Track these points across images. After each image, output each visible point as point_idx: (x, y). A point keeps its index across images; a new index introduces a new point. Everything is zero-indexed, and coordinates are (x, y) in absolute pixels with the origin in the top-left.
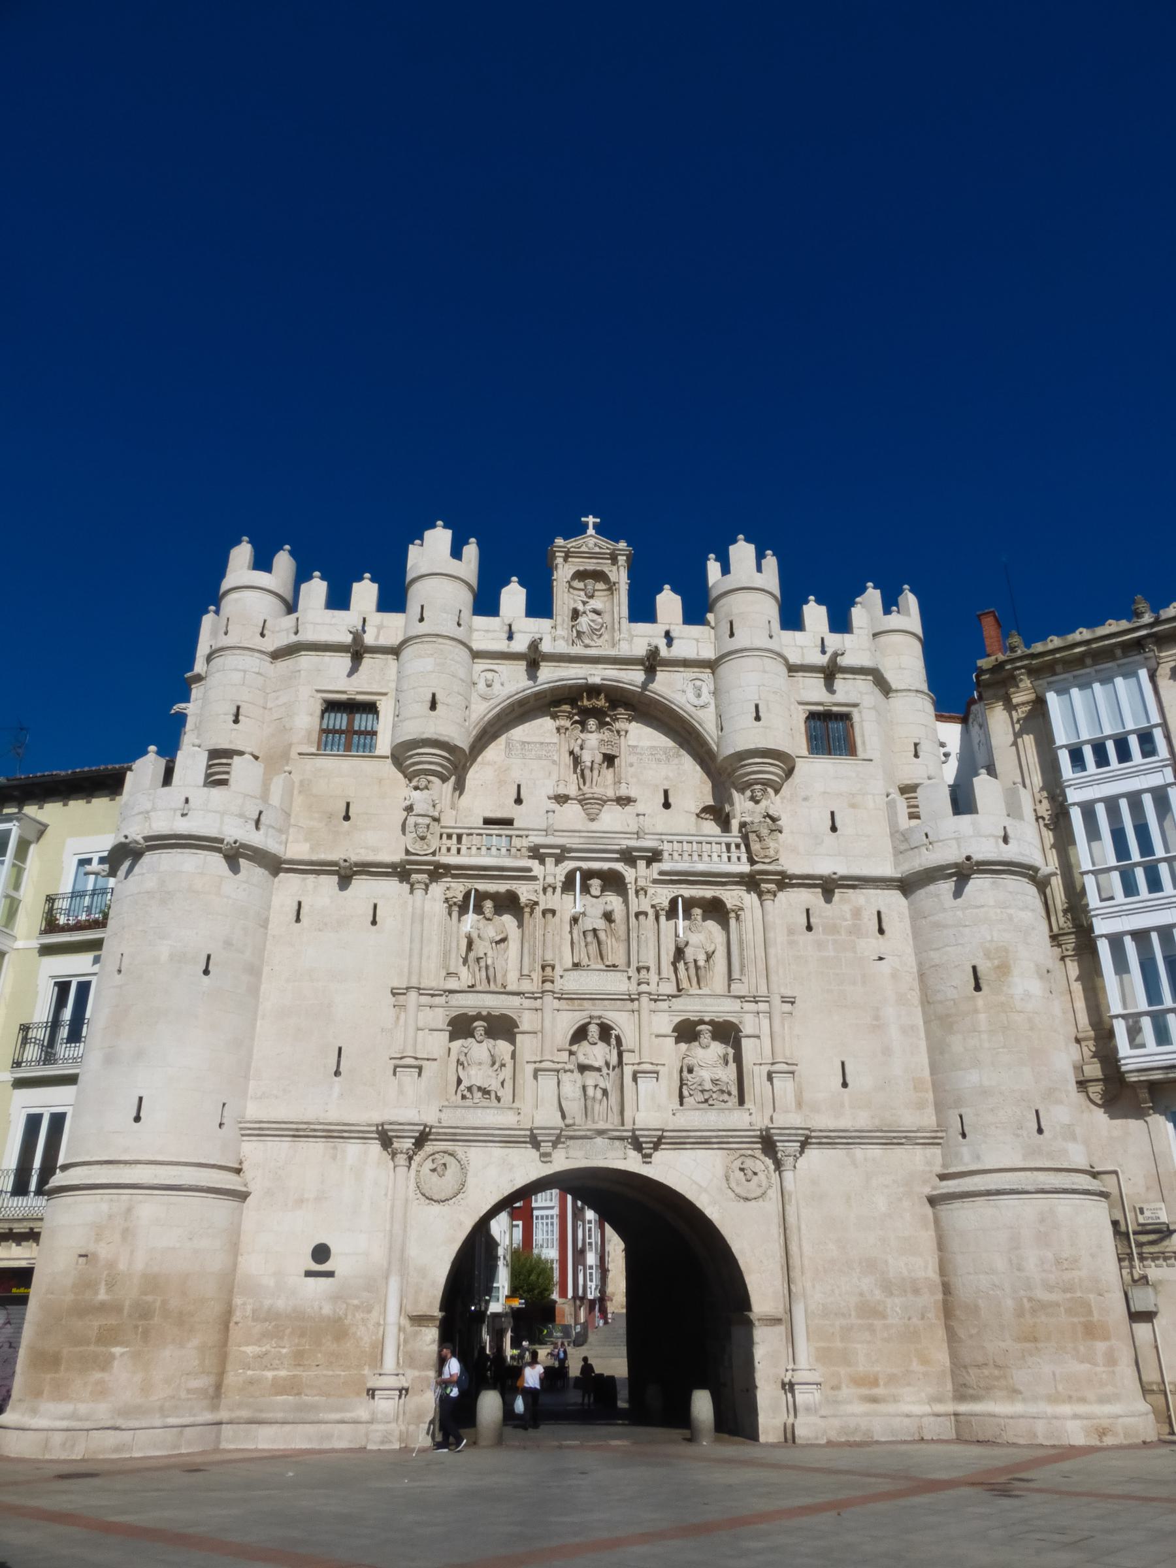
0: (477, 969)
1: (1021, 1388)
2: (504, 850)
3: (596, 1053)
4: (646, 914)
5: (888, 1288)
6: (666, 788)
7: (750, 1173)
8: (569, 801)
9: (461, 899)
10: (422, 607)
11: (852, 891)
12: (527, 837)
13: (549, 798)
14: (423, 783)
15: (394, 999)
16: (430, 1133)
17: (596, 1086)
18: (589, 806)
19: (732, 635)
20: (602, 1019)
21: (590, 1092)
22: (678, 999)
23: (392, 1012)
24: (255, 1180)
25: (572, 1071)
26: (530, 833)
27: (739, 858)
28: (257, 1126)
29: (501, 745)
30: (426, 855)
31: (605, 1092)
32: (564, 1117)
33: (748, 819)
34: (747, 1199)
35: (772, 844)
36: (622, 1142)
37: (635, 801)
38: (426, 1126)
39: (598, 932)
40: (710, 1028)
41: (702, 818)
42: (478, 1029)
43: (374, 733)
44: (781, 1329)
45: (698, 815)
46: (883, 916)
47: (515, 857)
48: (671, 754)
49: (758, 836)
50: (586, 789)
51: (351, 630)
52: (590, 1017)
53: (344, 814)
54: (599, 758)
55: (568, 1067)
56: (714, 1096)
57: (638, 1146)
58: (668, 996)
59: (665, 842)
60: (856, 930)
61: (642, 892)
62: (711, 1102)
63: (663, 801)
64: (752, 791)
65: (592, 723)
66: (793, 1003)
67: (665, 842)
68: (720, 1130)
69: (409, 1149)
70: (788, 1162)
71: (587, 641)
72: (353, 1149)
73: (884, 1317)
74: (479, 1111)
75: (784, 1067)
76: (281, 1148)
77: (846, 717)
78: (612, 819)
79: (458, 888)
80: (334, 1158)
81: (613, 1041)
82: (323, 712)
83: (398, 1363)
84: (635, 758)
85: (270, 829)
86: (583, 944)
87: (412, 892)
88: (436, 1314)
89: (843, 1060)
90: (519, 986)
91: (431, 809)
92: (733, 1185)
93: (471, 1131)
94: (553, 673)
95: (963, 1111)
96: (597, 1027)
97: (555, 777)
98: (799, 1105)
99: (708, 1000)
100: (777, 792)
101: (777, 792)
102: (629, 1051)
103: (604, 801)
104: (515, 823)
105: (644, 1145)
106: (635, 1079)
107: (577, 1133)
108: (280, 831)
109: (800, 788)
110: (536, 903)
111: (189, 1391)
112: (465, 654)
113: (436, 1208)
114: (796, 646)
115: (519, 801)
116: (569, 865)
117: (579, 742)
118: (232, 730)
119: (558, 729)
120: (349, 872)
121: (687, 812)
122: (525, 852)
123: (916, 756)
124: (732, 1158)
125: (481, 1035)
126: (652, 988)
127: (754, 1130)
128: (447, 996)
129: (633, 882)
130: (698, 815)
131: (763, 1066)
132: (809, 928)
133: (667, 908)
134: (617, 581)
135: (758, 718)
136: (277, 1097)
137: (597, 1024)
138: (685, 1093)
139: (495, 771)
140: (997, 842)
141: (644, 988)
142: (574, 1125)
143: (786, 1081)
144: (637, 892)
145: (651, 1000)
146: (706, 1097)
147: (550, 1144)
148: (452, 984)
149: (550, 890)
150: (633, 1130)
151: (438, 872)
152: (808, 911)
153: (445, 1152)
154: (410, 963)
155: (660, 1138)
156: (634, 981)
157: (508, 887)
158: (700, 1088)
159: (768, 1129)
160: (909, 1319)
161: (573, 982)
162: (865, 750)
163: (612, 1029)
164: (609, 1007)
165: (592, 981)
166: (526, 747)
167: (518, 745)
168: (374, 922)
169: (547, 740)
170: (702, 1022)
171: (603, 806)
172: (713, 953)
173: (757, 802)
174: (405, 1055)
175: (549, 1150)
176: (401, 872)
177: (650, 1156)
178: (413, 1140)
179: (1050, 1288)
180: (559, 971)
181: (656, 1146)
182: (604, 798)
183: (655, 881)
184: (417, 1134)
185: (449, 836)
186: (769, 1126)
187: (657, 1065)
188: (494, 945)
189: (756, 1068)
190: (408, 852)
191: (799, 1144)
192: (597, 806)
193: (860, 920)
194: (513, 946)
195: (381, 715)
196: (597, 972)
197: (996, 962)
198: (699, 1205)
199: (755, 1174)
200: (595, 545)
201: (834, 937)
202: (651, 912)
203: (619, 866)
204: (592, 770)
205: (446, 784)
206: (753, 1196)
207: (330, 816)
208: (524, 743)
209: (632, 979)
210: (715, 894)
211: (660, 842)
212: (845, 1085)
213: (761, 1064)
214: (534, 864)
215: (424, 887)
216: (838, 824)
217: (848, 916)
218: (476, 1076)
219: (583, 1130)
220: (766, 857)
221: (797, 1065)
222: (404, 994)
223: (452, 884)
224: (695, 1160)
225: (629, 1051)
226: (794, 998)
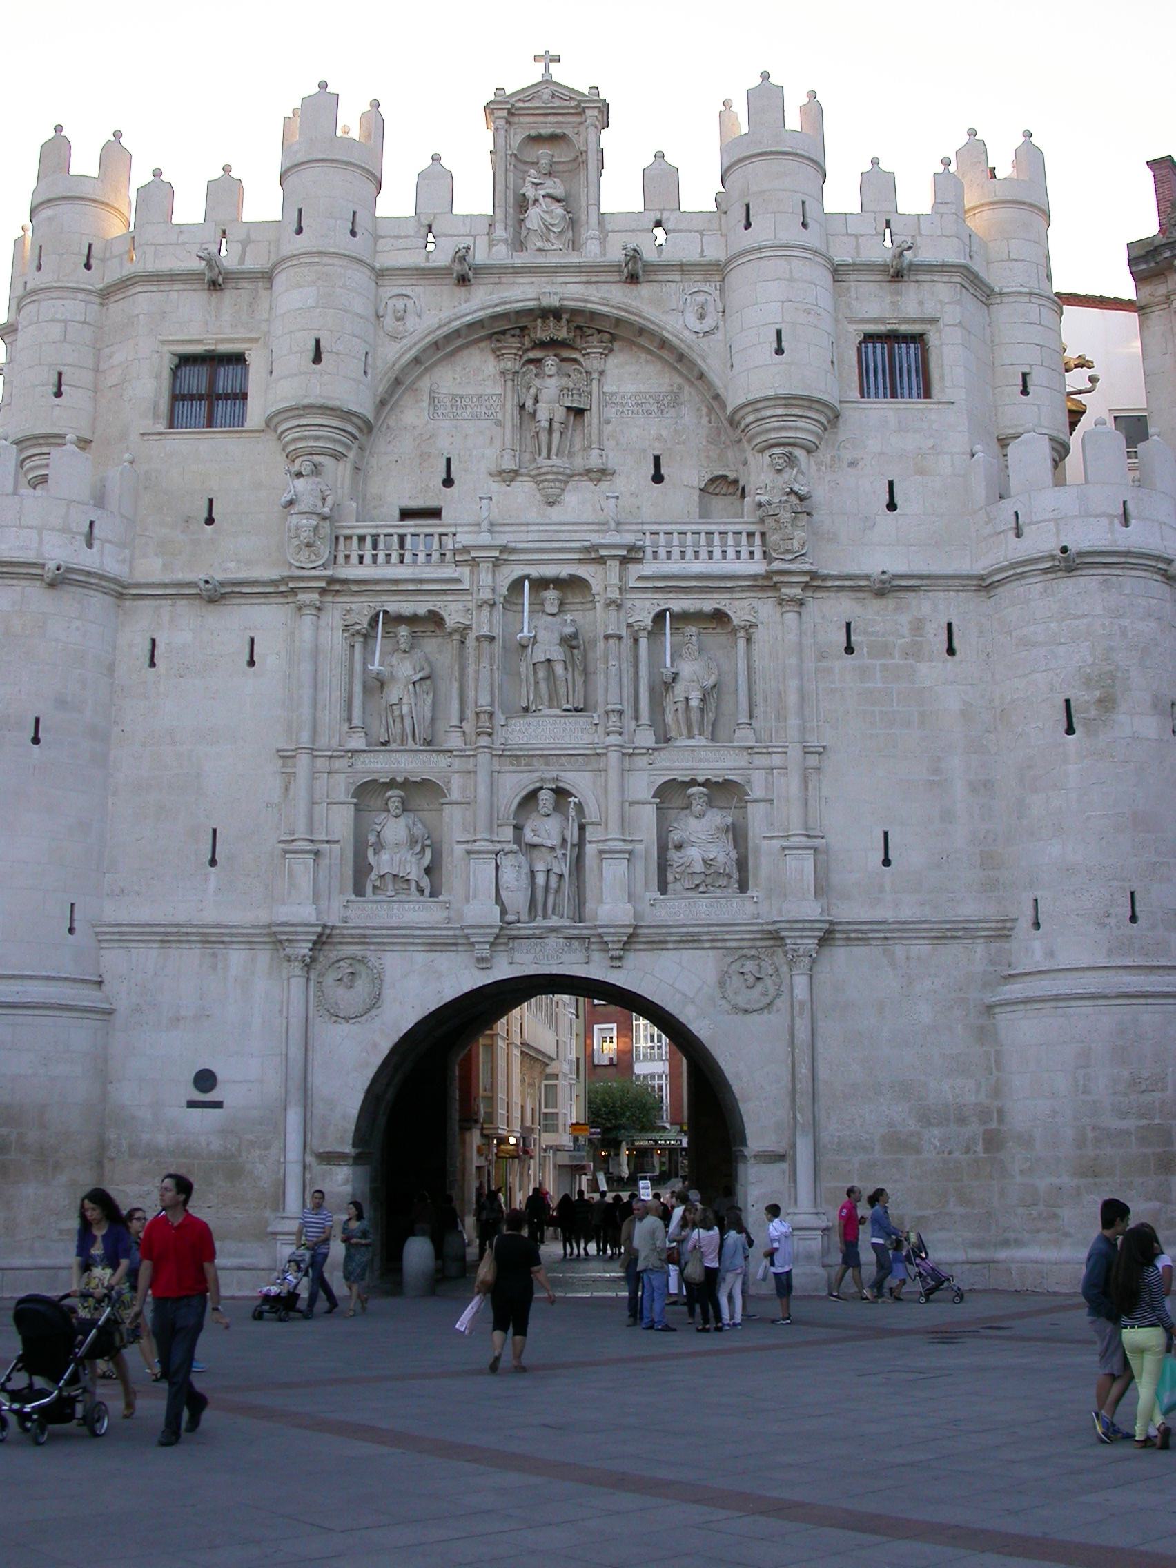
0: (391, 721)
1: (1072, 1231)
2: (422, 557)
4: (620, 638)
5: (926, 1118)
6: (657, 453)
7: (751, 979)
8: (520, 479)
9: (365, 626)
10: (300, 211)
11: (913, 594)
12: (455, 535)
13: (491, 475)
15: (280, 761)
19: (748, 225)
20: (561, 784)
21: (541, 879)
22: (662, 753)
23: (278, 782)
24: (121, 995)
26: (459, 529)
28: (116, 929)
29: (422, 400)
30: (314, 568)
31: (561, 876)
32: (504, 912)
33: (763, 499)
34: (746, 1011)
35: (799, 534)
38: (325, 926)
40: (704, 790)
42: (393, 799)
43: (244, 396)
44: (785, 1166)
46: (955, 629)
48: (665, 402)
49: (777, 521)
51: (200, 254)
52: (542, 780)
53: (205, 515)
54: (560, 414)
55: (507, 847)
56: (709, 880)
58: (648, 749)
59: (648, 534)
60: (915, 652)
62: (701, 889)
63: (652, 472)
65: (551, 363)
66: (820, 754)
67: (648, 534)
69: (304, 956)
70: (802, 964)
71: (539, 244)
72: (236, 957)
73: (918, 1151)
74: (396, 906)
76: (149, 956)
77: (918, 339)
80: (214, 968)
81: (572, 811)
82: (175, 372)
83: (304, 1206)
84: (614, 410)
85: (108, 545)
86: (532, 681)
88: (347, 1151)
89: (886, 829)
92: (730, 993)
93: (384, 932)
94: (491, 294)
95: (1039, 894)
97: (498, 443)
98: (822, 889)
101: (809, 451)
102: (593, 824)
103: (567, 478)
104: (443, 514)
107: (522, 932)
108: (123, 545)
110: (468, 627)
111: (61, 1232)
112: (361, 277)
113: (344, 1027)
114: (848, 234)
115: (448, 482)
117: (533, 391)
118: (53, 407)
119: (503, 373)
123: (1025, 392)
125: (397, 808)
128: (352, 757)
132: (849, 649)
133: (649, 628)
134: (584, 149)
135: (780, 351)
136: (138, 894)
138: (670, 878)
139: (414, 440)
140: (1111, 523)
142: (519, 922)
146: (697, 883)
147: (488, 947)
152: (848, 625)
153: (353, 958)
155: (631, 936)
156: (601, 729)
157: (430, 606)
160: (950, 1153)
162: (943, 390)
163: (571, 795)
164: (569, 767)
166: (459, 403)
167: (446, 400)
168: (251, 663)
169: (489, 391)
170: (693, 783)
171: (566, 482)
174: (295, 837)
175: (486, 954)
179: (1124, 1115)
180: (500, 718)
182: (568, 471)
184: (315, 938)
188: (411, 687)
191: (816, 942)
192: (557, 484)
193: (922, 636)
195: (252, 370)
197: (1097, 693)
198: (682, 1019)
199: (758, 979)
200: (553, 96)
201: (883, 661)
202: (624, 632)
203: (583, 571)
204: (550, 431)
206: (757, 1006)
207: (187, 520)
208: (454, 397)
209: (599, 727)
210: (718, 606)
211: (640, 536)
212: (887, 862)
213: (772, 837)
216: (897, 500)
220: (787, 552)
221: (823, 837)
222: (294, 757)
223: (354, 606)
224: (680, 964)
225: (593, 824)
226: (824, 747)
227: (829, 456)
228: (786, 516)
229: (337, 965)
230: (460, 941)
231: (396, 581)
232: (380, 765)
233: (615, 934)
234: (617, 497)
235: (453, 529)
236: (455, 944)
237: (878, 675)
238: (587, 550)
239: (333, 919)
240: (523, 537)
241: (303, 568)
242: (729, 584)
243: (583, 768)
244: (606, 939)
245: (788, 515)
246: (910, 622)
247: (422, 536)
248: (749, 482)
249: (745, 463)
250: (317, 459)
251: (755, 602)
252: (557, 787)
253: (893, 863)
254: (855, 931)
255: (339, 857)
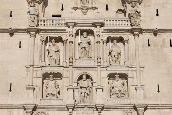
3: (85, 83)
6: (107, 4)
11: (163, 34)
12: (64, 20)
13: (72, 8)
14: (32, 5)
15: (26, 69)
16: (36, 107)
17: (85, 93)
18: (83, 10)
23: (26, 73)
25: (78, 89)
26: (65, 19)
27: (128, 25)
31: (88, 94)
33: (130, 13)
35: (138, 20)
36: (92, 108)
37: (98, 8)
38: (35, 105)
39: (86, 48)
40: (118, 75)
41: (118, 13)
45: (116, 12)
47: (61, 26)
49: (133, 18)
50: (82, 5)
53: (10, 15)
55: (76, 87)
56: (120, 95)
57: (97, 110)
60: (163, 46)
61: (98, 36)
62: (118, 97)
64: (132, 4)
68: (121, 105)
72: (15, 112)
74: (51, 100)
75: (140, 86)
78: (91, 14)
79: (44, 36)
81: (90, 79)
87: (31, 37)
89: (158, 84)
90: (63, 64)
91: (35, 12)
96: (85, 76)
98: (145, 97)
99: (118, 67)
100: (140, 4)
101: (140, 4)
103: (88, 9)
105: (99, 109)
106: (96, 90)
109: (147, 3)
110: (67, 40)
116: (77, 28)
120: (12, 32)
121: (113, 11)
122: (63, 24)
124: (125, 113)
126: (102, 64)
127: (131, 105)
128: (42, 68)
129: (96, 33)
130: (116, 12)
131: (134, 86)
132: (149, 45)
133: (106, 40)
137: (85, 75)
141: (99, 64)
142: (78, 104)
143: (140, 90)
144: (97, 36)
145: (101, 67)
148: (43, 64)
149: (71, 36)
150: (95, 105)
151: (38, 31)
152: (149, 40)
153: (42, 112)
154: (31, 58)
155: (103, 107)
156: (96, 62)
157: (59, 35)
158: (115, 93)
159: (135, 104)
161: (78, 63)
163: (90, 76)
165: (85, 62)
168: (20, 47)
170: (116, 74)
171: (88, 10)
172: (120, 53)
173: (133, 7)
175: (71, 111)
176: (27, 31)
177: (101, 112)
178: (32, 109)
180: (74, 60)
181: (102, 109)
183: (103, 32)
184: (33, 107)
185: (41, 21)
186: (135, 103)
187: (103, 86)
188: (55, 52)
189: (132, 87)
190: (29, 26)
191: (144, 109)
194: (62, 52)
196: (85, 60)
202: (101, 42)
203: (92, 28)
205: (40, 5)
207: (6, 16)
211: (104, 21)
212: (159, 91)
214: (67, 28)
215: (34, 36)
216: (159, 13)
217: (161, 41)
218: (52, 90)
219: (81, 105)
222: (29, 67)
224: (114, 113)
227: (144, 4)
228: (135, 16)
229: (38, 114)
230: (65, 108)
231: (52, 30)
232: (48, 70)
233: (99, 107)
234: (99, 12)
235: (64, 19)
236: (65, 109)
237: (155, 51)
238: (92, 24)
239: (37, 103)
240: (79, 21)
241: (32, 26)
242: (123, 31)
243: (92, 70)
244: (98, 108)
245: (136, 16)
246: (162, 40)
247: (57, 20)
248: (127, 10)
249: (126, 6)
250: (35, 3)
251: (128, 35)
252: (87, 74)
253: (160, 92)
254: (152, 107)
255: (38, 90)
